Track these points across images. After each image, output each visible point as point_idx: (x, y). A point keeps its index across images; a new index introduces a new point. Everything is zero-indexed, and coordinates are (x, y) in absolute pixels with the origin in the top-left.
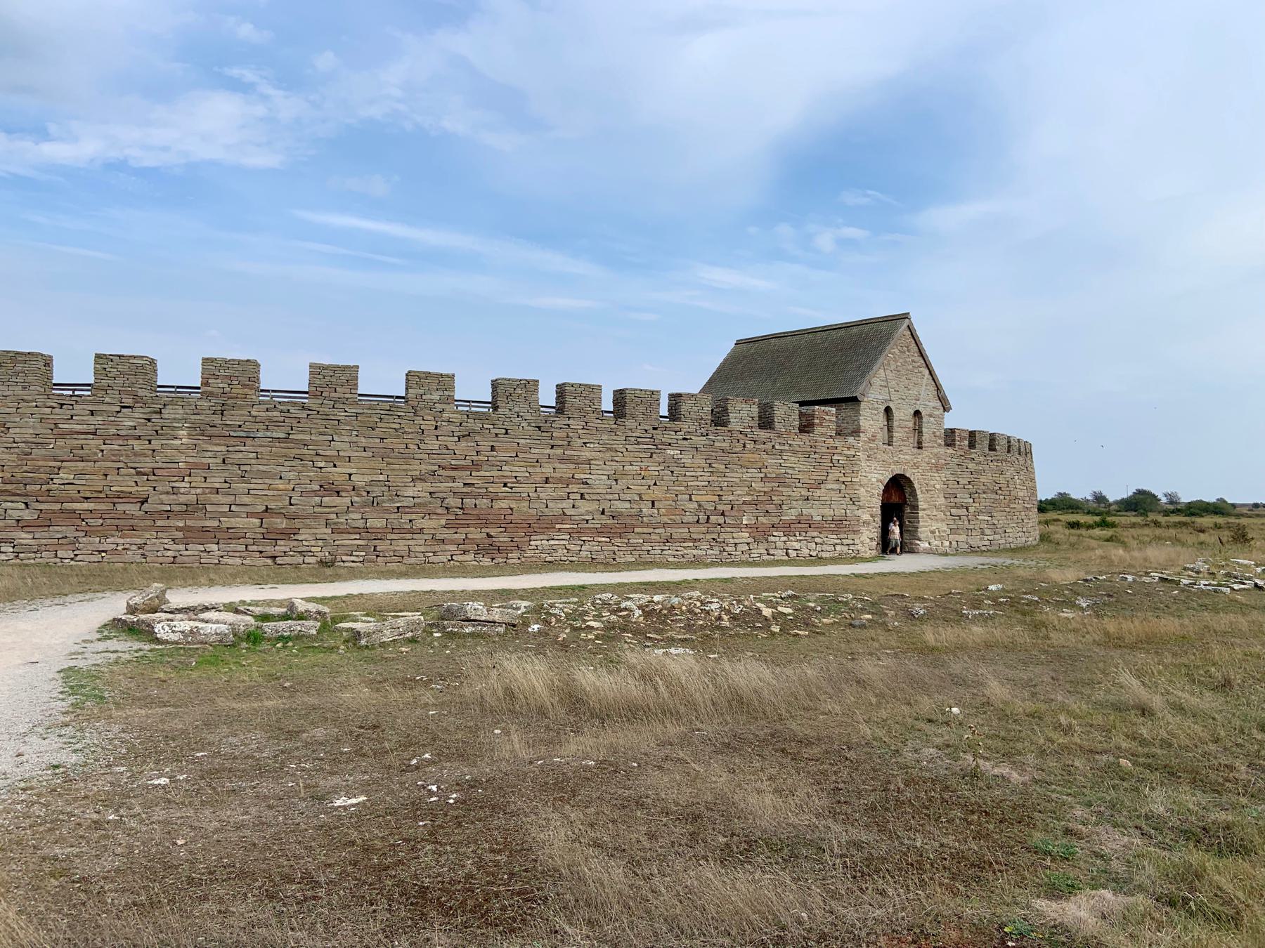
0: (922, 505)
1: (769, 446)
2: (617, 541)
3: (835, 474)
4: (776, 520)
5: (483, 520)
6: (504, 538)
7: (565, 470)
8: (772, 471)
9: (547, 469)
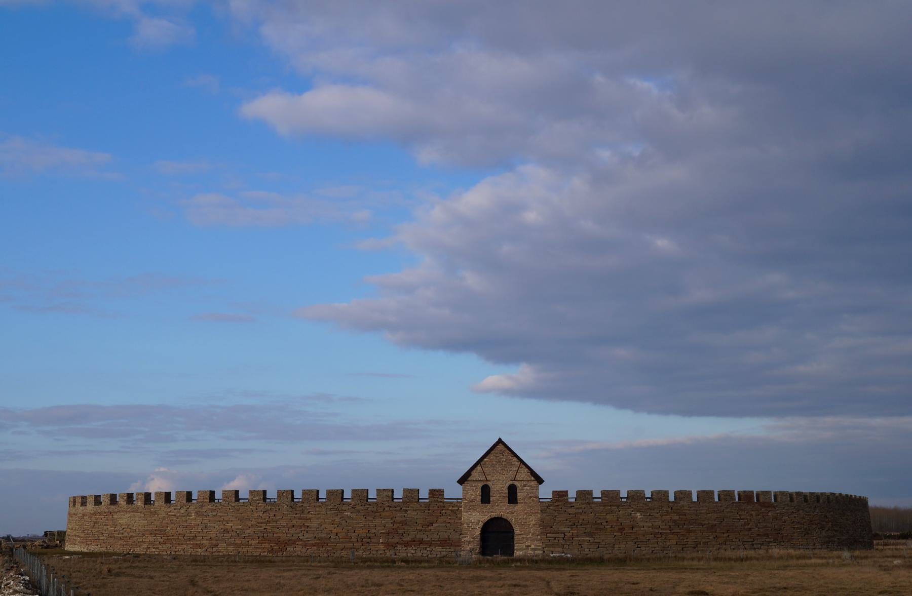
1: (398, 508)
2: (321, 549)
3: (441, 519)
5: (270, 541)
8: (398, 519)
9: (294, 522)
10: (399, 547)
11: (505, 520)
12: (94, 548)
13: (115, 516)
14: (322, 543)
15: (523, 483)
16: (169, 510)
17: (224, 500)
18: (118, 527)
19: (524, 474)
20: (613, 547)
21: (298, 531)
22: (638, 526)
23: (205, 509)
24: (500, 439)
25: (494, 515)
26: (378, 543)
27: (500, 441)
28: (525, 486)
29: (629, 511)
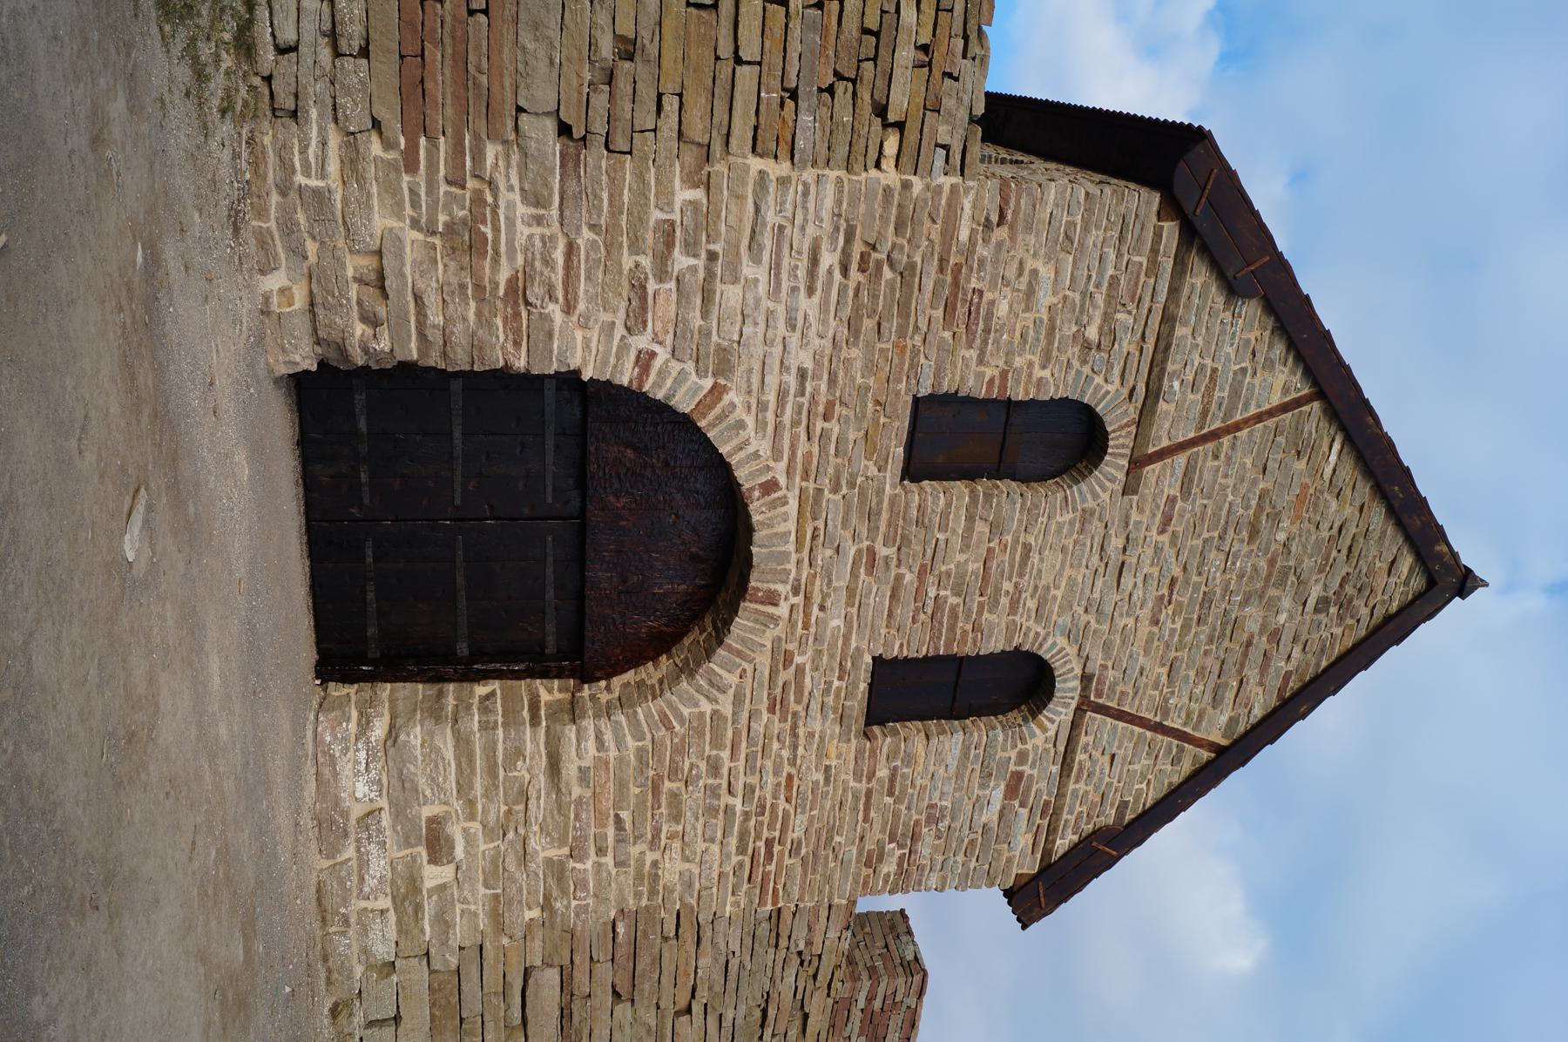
0: (583, 746)
19: (1123, 769)
24: (1465, 583)
25: (775, 527)
27: (1443, 579)
28: (1015, 786)
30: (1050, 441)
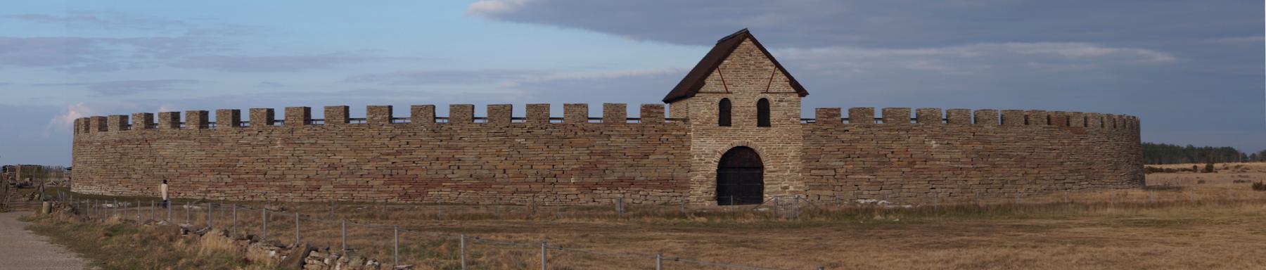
1: (597, 133)
2: (481, 193)
3: (661, 149)
4: (597, 180)
5: (402, 181)
6: (412, 191)
7: (448, 154)
9: (438, 153)
10: (600, 191)
11: (752, 150)
12: (121, 190)
13: (154, 145)
14: (482, 184)
15: (780, 96)
16: (240, 136)
17: (327, 121)
18: (159, 161)
19: (780, 83)
20: (901, 188)
21: (446, 166)
22: (933, 159)
23: (297, 133)
25: (737, 143)
26: (568, 184)
29: (921, 137)
30: (725, 107)
